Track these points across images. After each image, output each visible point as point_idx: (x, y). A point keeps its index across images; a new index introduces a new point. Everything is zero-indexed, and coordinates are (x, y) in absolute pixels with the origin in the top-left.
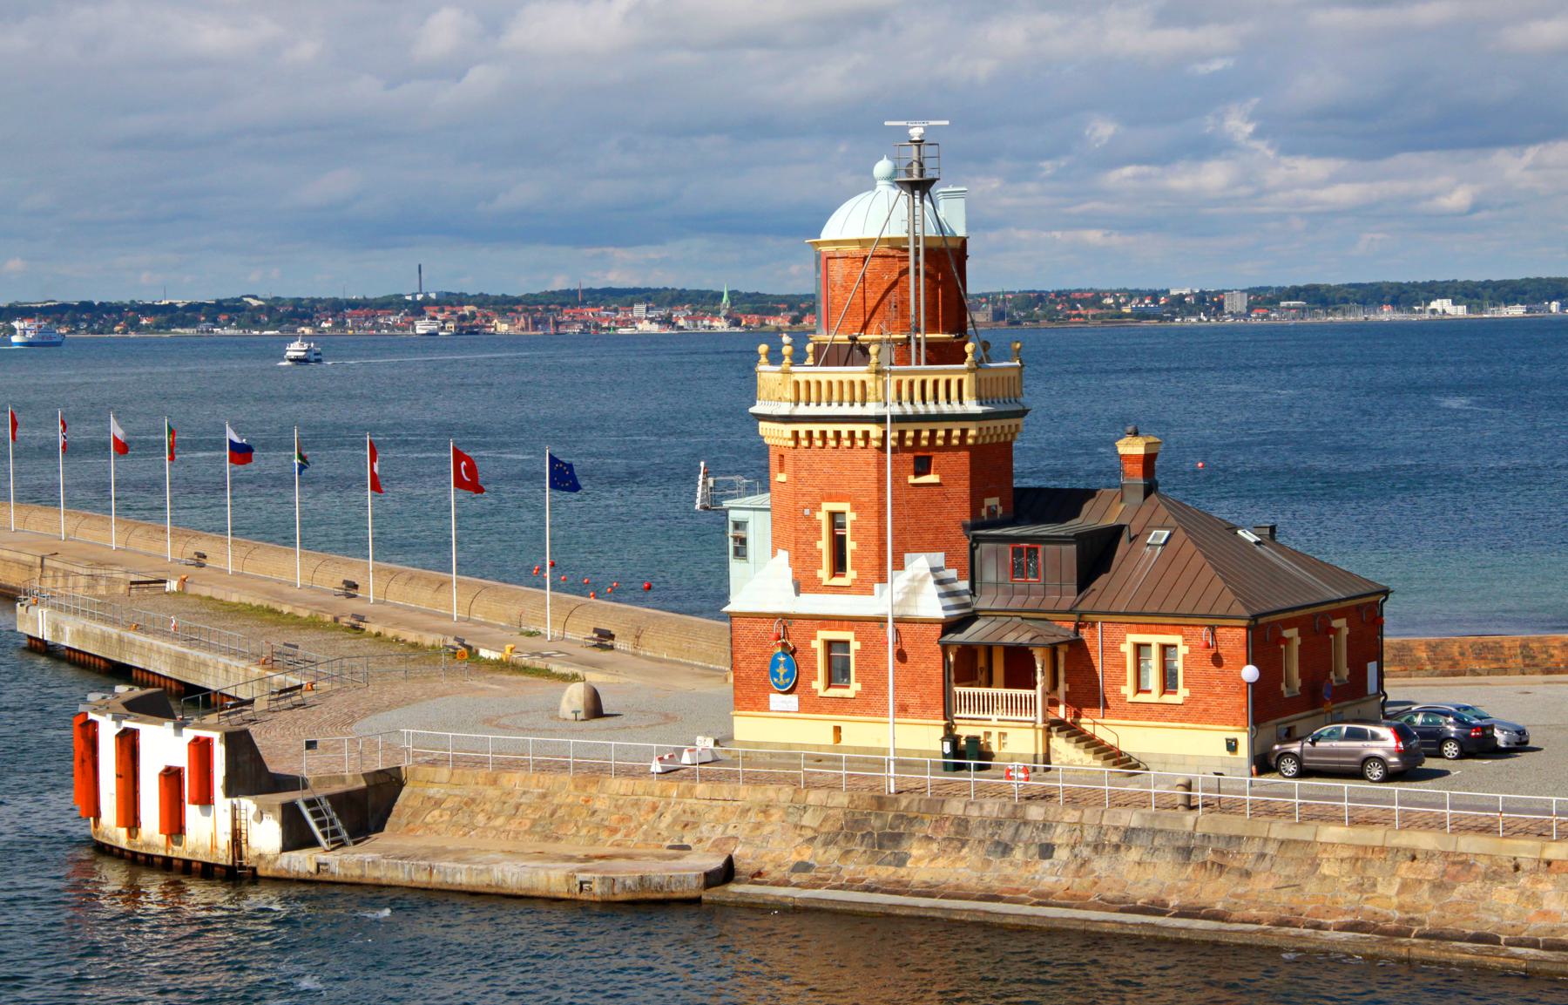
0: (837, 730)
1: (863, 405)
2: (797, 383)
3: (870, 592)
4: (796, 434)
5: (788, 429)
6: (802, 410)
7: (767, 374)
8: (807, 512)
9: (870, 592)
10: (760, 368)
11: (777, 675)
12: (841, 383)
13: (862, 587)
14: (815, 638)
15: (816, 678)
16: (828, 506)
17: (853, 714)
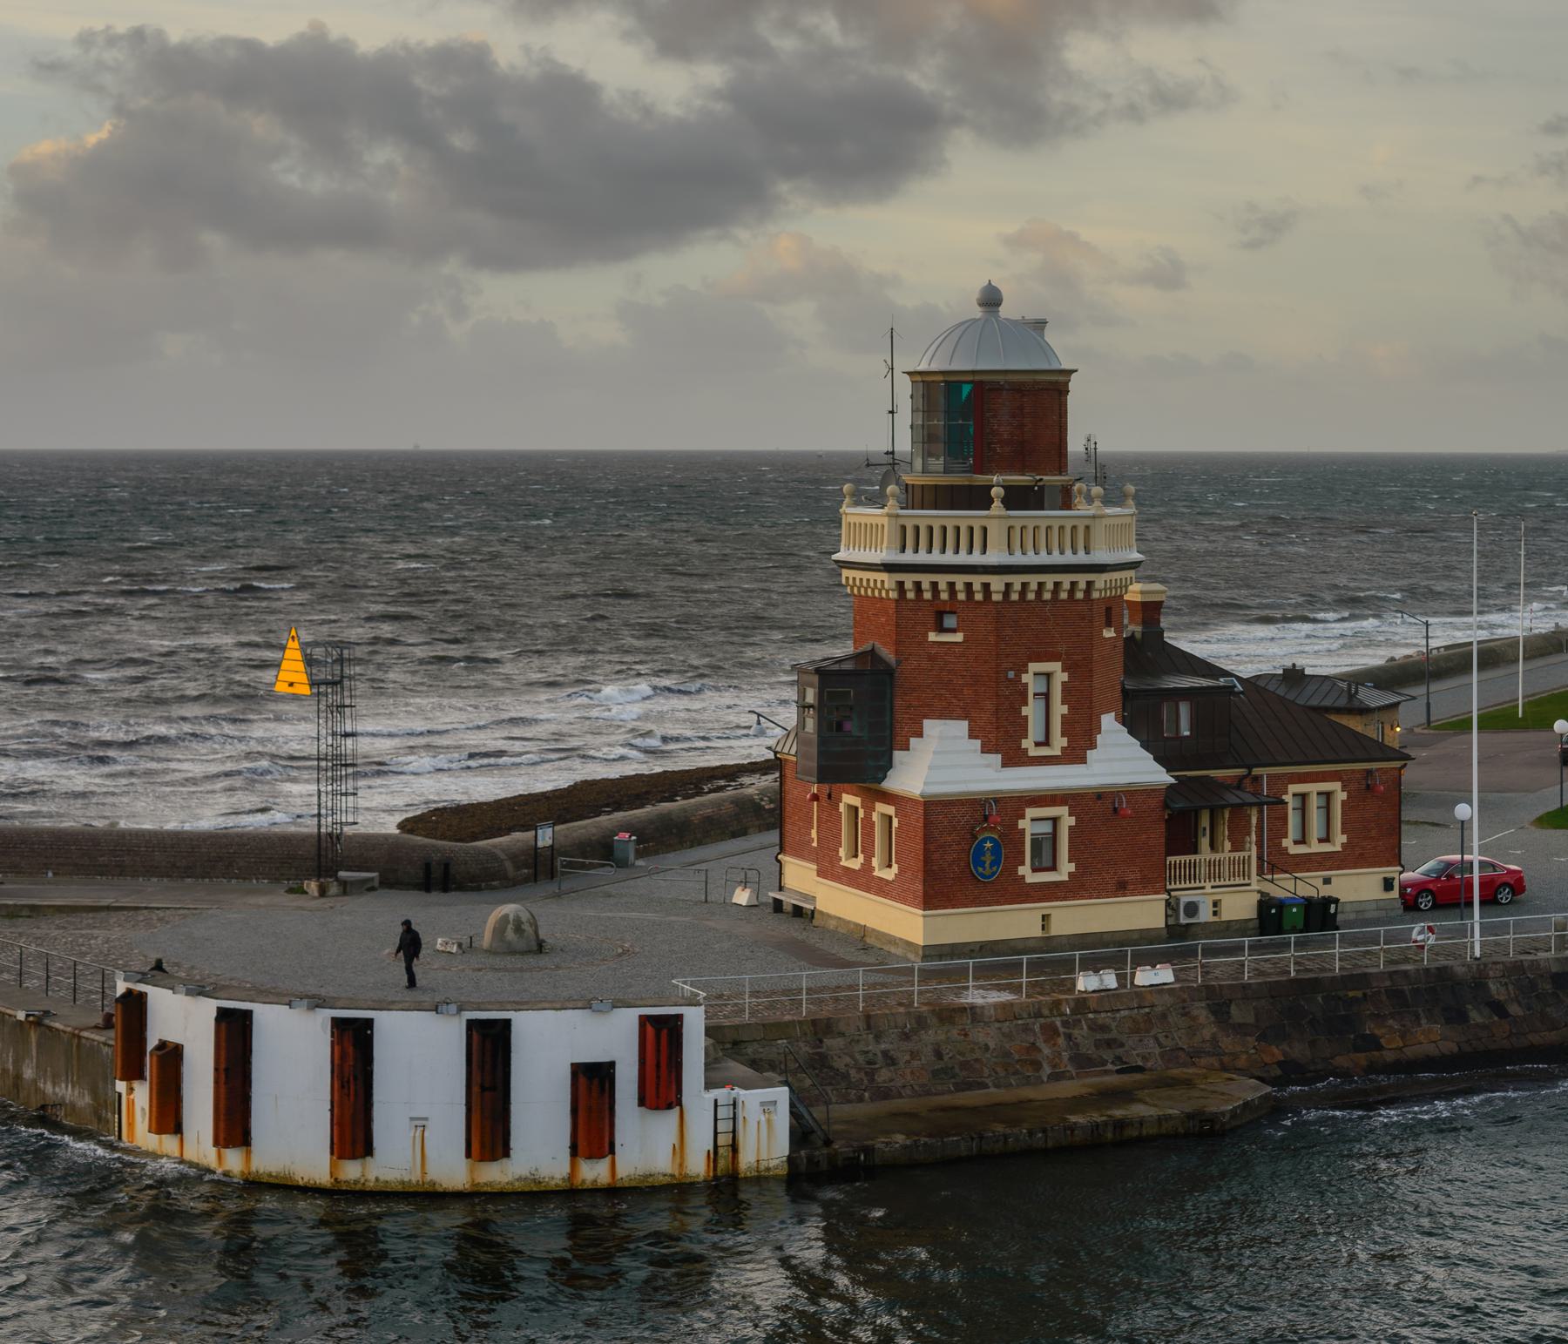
0: (1045, 918)
1: (984, 552)
2: (904, 528)
3: (1082, 760)
4: (901, 584)
5: (997, 583)
6: (1018, 559)
7: (852, 514)
8: (1011, 674)
9: (1082, 760)
10: (844, 509)
11: (983, 864)
12: (917, 529)
13: (1075, 755)
14: (1023, 817)
15: (1023, 863)
16: (1034, 667)
17: (1065, 899)
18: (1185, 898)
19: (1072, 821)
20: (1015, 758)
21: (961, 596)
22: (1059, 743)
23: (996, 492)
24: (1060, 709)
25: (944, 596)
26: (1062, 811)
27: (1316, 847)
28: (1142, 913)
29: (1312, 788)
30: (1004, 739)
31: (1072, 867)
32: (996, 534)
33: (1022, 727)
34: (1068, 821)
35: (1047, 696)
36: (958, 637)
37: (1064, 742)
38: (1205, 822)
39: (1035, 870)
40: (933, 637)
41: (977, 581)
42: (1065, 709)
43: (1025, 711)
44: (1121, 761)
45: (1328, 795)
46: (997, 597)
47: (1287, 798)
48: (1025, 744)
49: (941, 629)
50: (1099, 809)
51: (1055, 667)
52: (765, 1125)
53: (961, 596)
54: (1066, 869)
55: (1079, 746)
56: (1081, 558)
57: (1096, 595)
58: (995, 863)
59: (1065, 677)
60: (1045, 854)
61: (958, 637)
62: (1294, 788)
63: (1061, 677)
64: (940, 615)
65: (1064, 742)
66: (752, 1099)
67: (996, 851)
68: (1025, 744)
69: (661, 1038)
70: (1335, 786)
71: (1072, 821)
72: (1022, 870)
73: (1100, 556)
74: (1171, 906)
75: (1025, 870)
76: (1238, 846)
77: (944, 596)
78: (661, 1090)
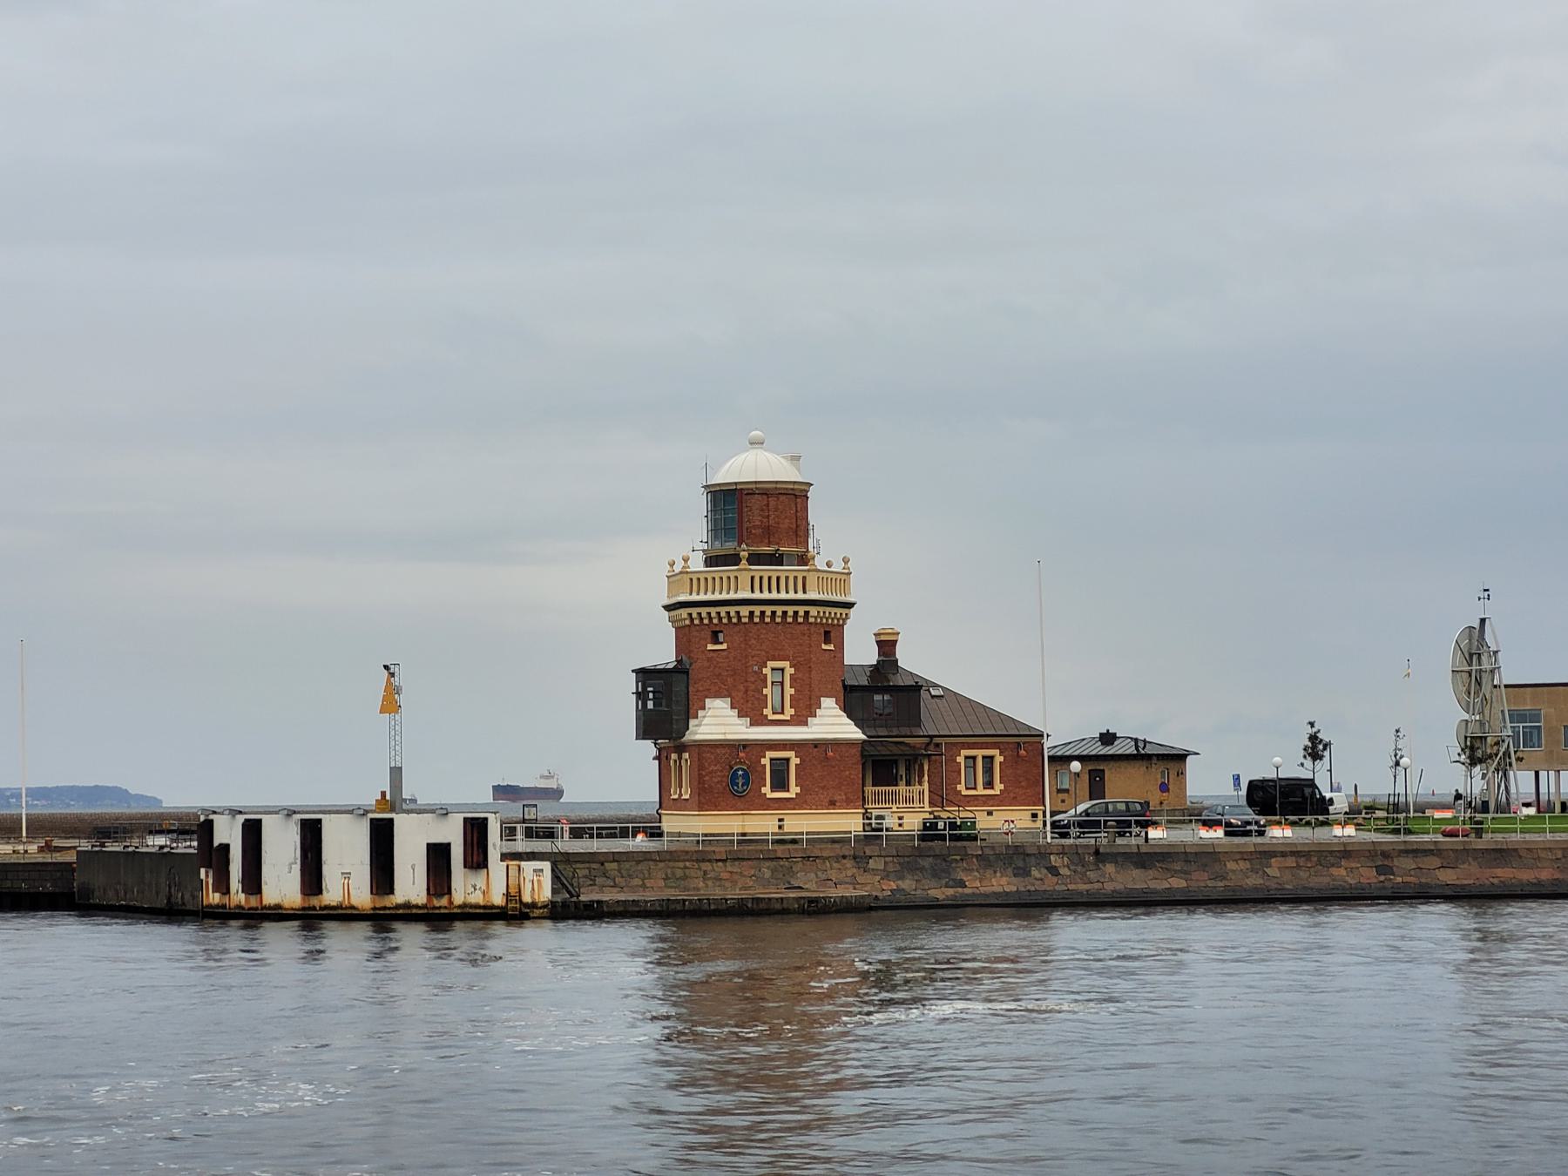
5: (744, 611)
6: (757, 595)
13: (800, 720)
16: (771, 664)
18: (875, 813)
19: (798, 761)
20: (759, 720)
21: (725, 621)
22: (789, 712)
23: (744, 554)
24: (789, 691)
25: (715, 621)
26: (791, 754)
27: (981, 791)
28: (849, 822)
29: (979, 753)
30: (752, 710)
31: (798, 790)
32: (744, 578)
33: (763, 701)
34: (795, 761)
35: (782, 683)
36: (724, 646)
37: (792, 712)
38: (902, 771)
39: (774, 788)
40: (710, 647)
41: (732, 610)
42: (792, 691)
43: (765, 691)
44: (833, 723)
45: (989, 760)
46: (745, 620)
47: (960, 759)
48: (765, 712)
49: (716, 642)
50: (813, 750)
51: (786, 664)
52: (538, 883)
53: (725, 621)
54: (794, 791)
55: (805, 711)
56: (800, 596)
57: (812, 620)
58: (746, 784)
59: (792, 671)
60: (780, 783)
61: (724, 646)
62: (964, 752)
63: (790, 671)
64: (715, 634)
65: (792, 712)
66: (529, 866)
67: (746, 775)
68: (765, 712)
69: (476, 830)
70: (995, 752)
71: (798, 761)
72: (764, 790)
73: (812, 595)
74: (866, 816)
75: (766, 790)
76: (920, 783)
77: (715, 621)
78: (477, 858)
